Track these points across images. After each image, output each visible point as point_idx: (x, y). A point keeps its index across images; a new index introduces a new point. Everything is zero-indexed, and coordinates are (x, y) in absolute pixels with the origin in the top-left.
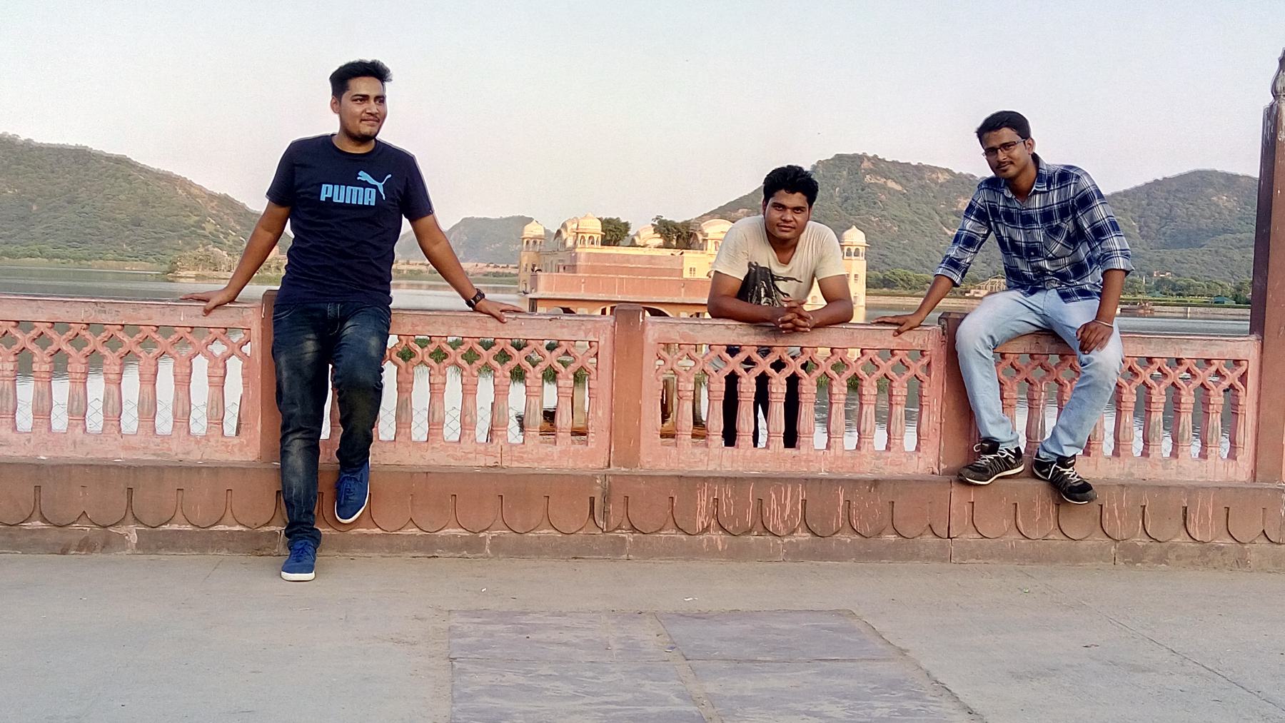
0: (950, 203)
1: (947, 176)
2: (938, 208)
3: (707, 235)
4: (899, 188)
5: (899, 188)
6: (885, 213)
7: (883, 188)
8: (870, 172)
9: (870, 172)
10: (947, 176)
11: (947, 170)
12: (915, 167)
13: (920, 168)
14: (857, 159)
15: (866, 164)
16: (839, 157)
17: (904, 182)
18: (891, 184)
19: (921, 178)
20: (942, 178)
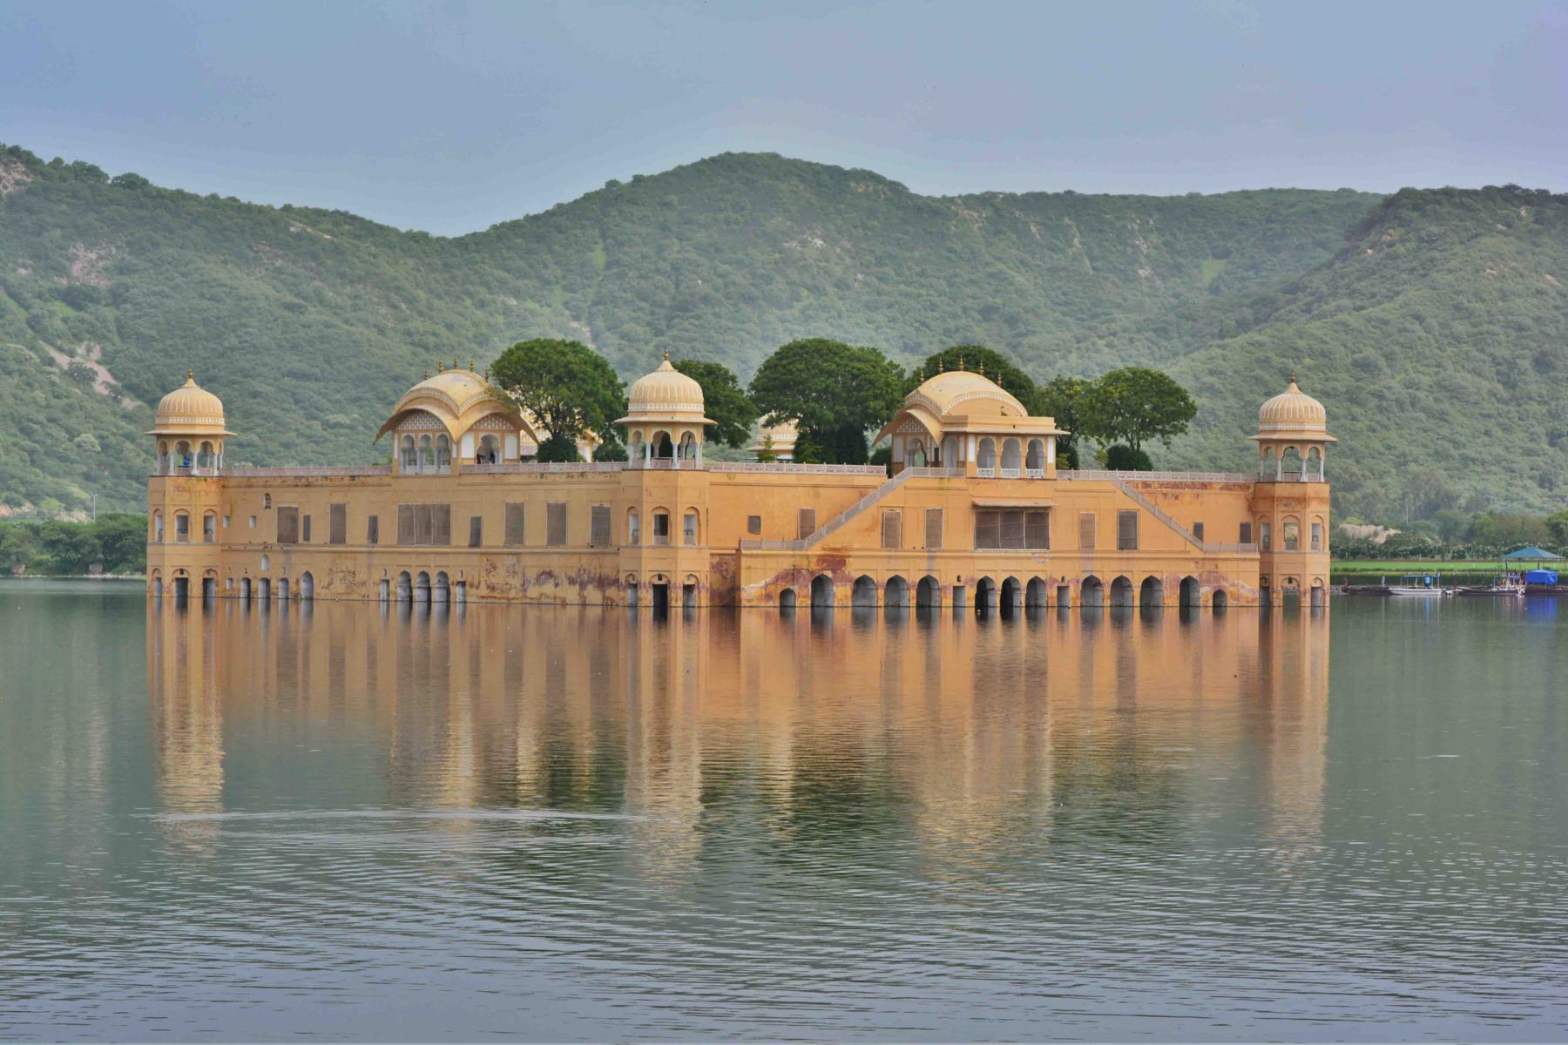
2: (11, 278)
10: (19, 173)
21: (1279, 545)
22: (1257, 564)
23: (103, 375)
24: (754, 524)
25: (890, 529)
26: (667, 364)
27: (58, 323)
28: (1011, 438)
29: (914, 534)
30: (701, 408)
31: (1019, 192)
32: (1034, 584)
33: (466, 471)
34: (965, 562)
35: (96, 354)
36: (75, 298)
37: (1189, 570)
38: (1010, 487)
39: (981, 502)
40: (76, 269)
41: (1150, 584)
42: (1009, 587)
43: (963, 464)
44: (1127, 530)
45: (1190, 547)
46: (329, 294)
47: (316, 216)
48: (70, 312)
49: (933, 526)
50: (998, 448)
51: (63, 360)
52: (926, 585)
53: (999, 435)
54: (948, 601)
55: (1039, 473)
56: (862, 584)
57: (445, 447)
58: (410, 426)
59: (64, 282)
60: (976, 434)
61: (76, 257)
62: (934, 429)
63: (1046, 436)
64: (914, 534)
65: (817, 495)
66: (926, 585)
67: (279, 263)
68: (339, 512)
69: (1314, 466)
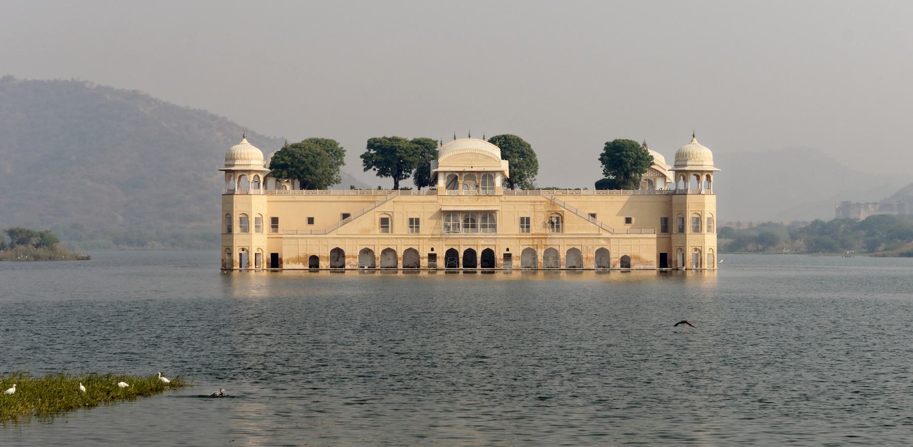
21: (675, 229)
22: (654, 242)
24: (311, 221)
25: (385, 223)
26: (245, 140)
28: (471, 175)
29: (400, 226)
38: (465, 200)
39: (444, 209)
41: (574, 252)
42: (470, 254)
44: (556, 223)
49: (414, 223)
52: (412, 253)
53: (461, 173)
56: (367, 252)
60: (445, 172)
63: (495, 172)
64: (400, 226)
66: (412, 253)
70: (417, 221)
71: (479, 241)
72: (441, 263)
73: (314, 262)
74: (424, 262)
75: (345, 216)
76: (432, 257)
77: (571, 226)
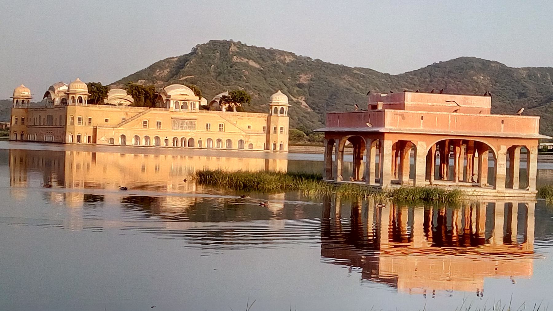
0: (294, 78)
1: (292, 58)
2: (285, 81)
3: (170, 96)
4: (257, 66)
5: (257, 66)
6: (248, 84)
7: (247, 66)
8: (237, 54)
9: (237, 54)
11: (291, 53)
12: (268, 50)
13: (272, 52)
14: (226, 44)
15: (233, 48)
16: (213, 43)
17: (261, 62)
18: (251, 63)
19: (273, 59)
20: (288, 59)
23: (304, 103)
24: (107, 120)
27: (295, 91)
30: (87, 90)
31: (536, 67)
32: (191, 140)
33: (56, 107)
34: (169, 133)
35: (303, 99)
36: (300, 86)
37: (242, 138)
40: (301, 80)
43: (169, 108)
45: (241, 132)
46: (361, 87)
47: (361, 69)
48: (298, 89)
50: (181, 103)
51: (295, 100)
54: (163, 144)
55: (193, 111)
57: (53, 102)
58: (49, 96)
59: (298, 82)
61: (300, 78)
62: (164, 98)
65: (127, 114)
67: (350, 79)
68: (40, 116)
69: (282, 112)
70: (160, 122)
71: (188, 134)
72: (171, 144)
73: (112, 139)
74: (163, 144)
75: (124, 119)
76: (166, 140)
77: (228, 128)
